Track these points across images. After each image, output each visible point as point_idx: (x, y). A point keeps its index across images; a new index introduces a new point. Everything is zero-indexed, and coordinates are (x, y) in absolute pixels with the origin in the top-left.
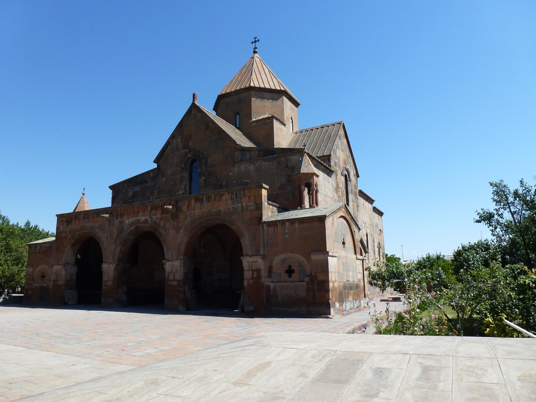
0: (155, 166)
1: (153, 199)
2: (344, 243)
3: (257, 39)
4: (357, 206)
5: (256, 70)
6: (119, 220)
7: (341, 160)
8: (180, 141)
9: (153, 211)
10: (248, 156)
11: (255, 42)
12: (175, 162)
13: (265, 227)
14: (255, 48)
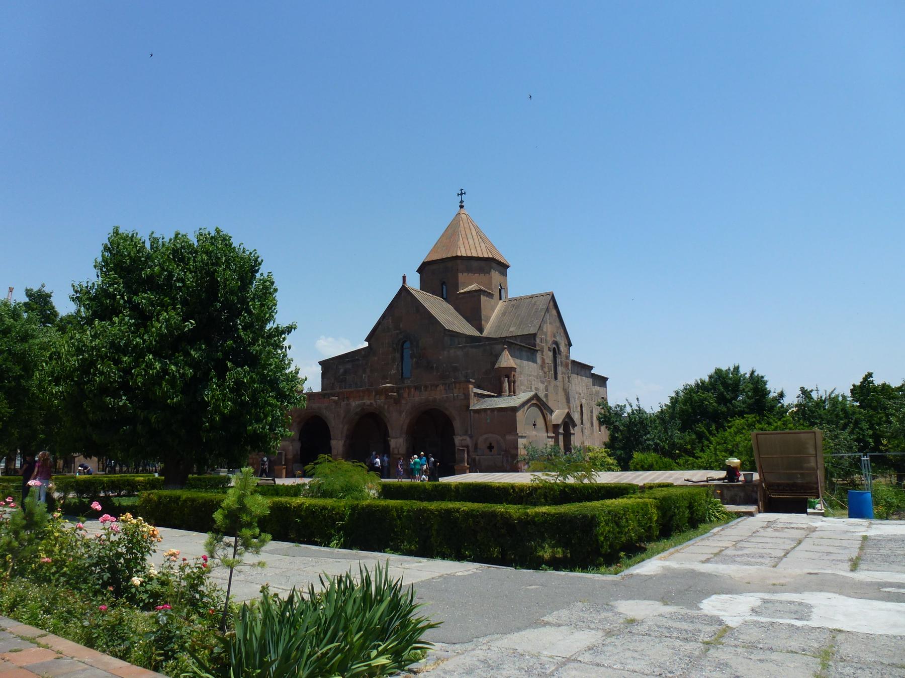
0: (366, 344)
2: (534, 425)
3: (463, 192)
4: (568, 377)
5: (463, 233)
6: (345, 402)
7: (549, 334)
9: (378, 396)
11: (461, 194)
13: (472, 414)
14: (462, 202)
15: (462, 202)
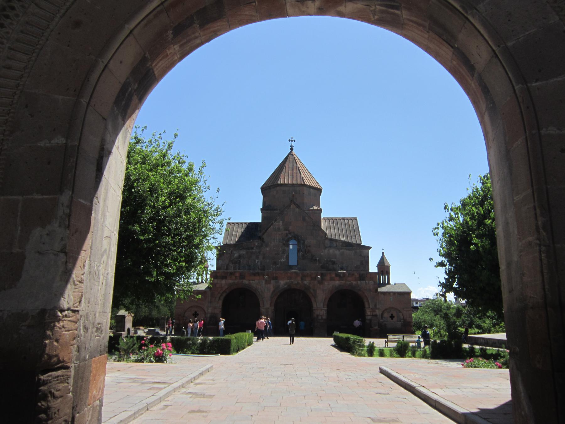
1: (258, 262)
5: (300, 168)
8: (281, 225)
10: (335, 245)
11: (292, 141)
12: (277, 238)
14: (292, 146)
15: (292, 146)
